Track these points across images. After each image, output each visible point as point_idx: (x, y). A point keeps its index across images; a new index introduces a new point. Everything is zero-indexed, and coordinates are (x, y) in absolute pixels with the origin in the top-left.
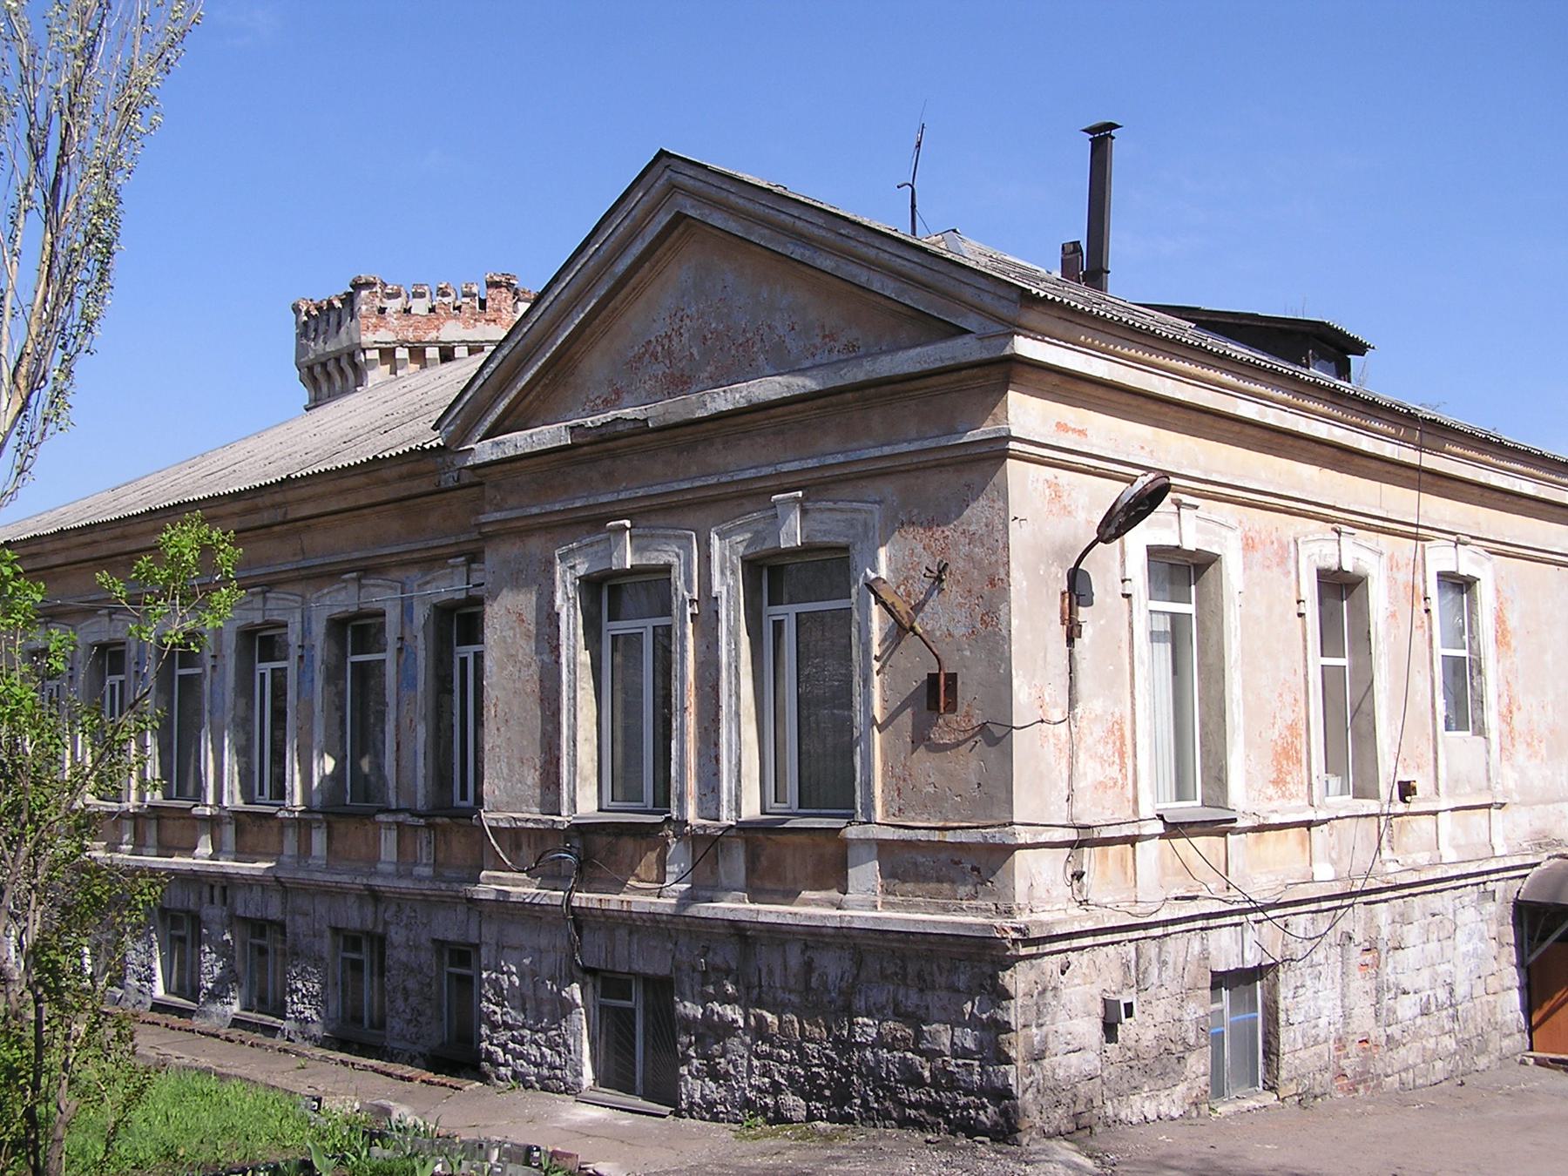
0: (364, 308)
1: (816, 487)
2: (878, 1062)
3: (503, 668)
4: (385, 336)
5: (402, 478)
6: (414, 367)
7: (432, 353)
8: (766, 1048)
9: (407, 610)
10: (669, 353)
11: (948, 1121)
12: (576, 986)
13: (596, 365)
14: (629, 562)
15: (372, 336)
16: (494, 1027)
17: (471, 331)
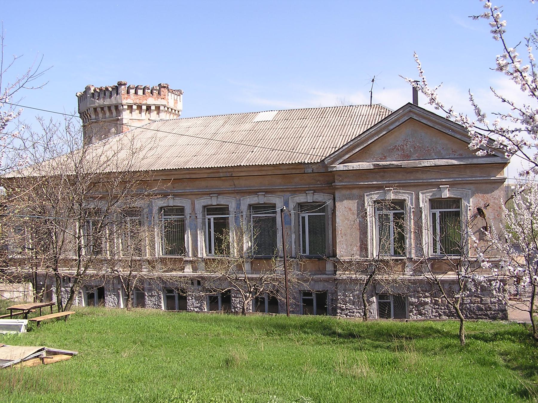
0: (123, 92)
1: (452, 185)
2: (471, 307)
3: (343, 222)
4: (130, 101)
5: (288, 169)
6: (138, 111)
7: (144, 107)
8: (437, 307)
9: (286, 204)
10: (403, 150)
11: (489, 317)
12: (374, 298)
13: (377, 149)
14: (392, 197)
15: (126, 101)
16: (343, 310)
17: (157, 101)
